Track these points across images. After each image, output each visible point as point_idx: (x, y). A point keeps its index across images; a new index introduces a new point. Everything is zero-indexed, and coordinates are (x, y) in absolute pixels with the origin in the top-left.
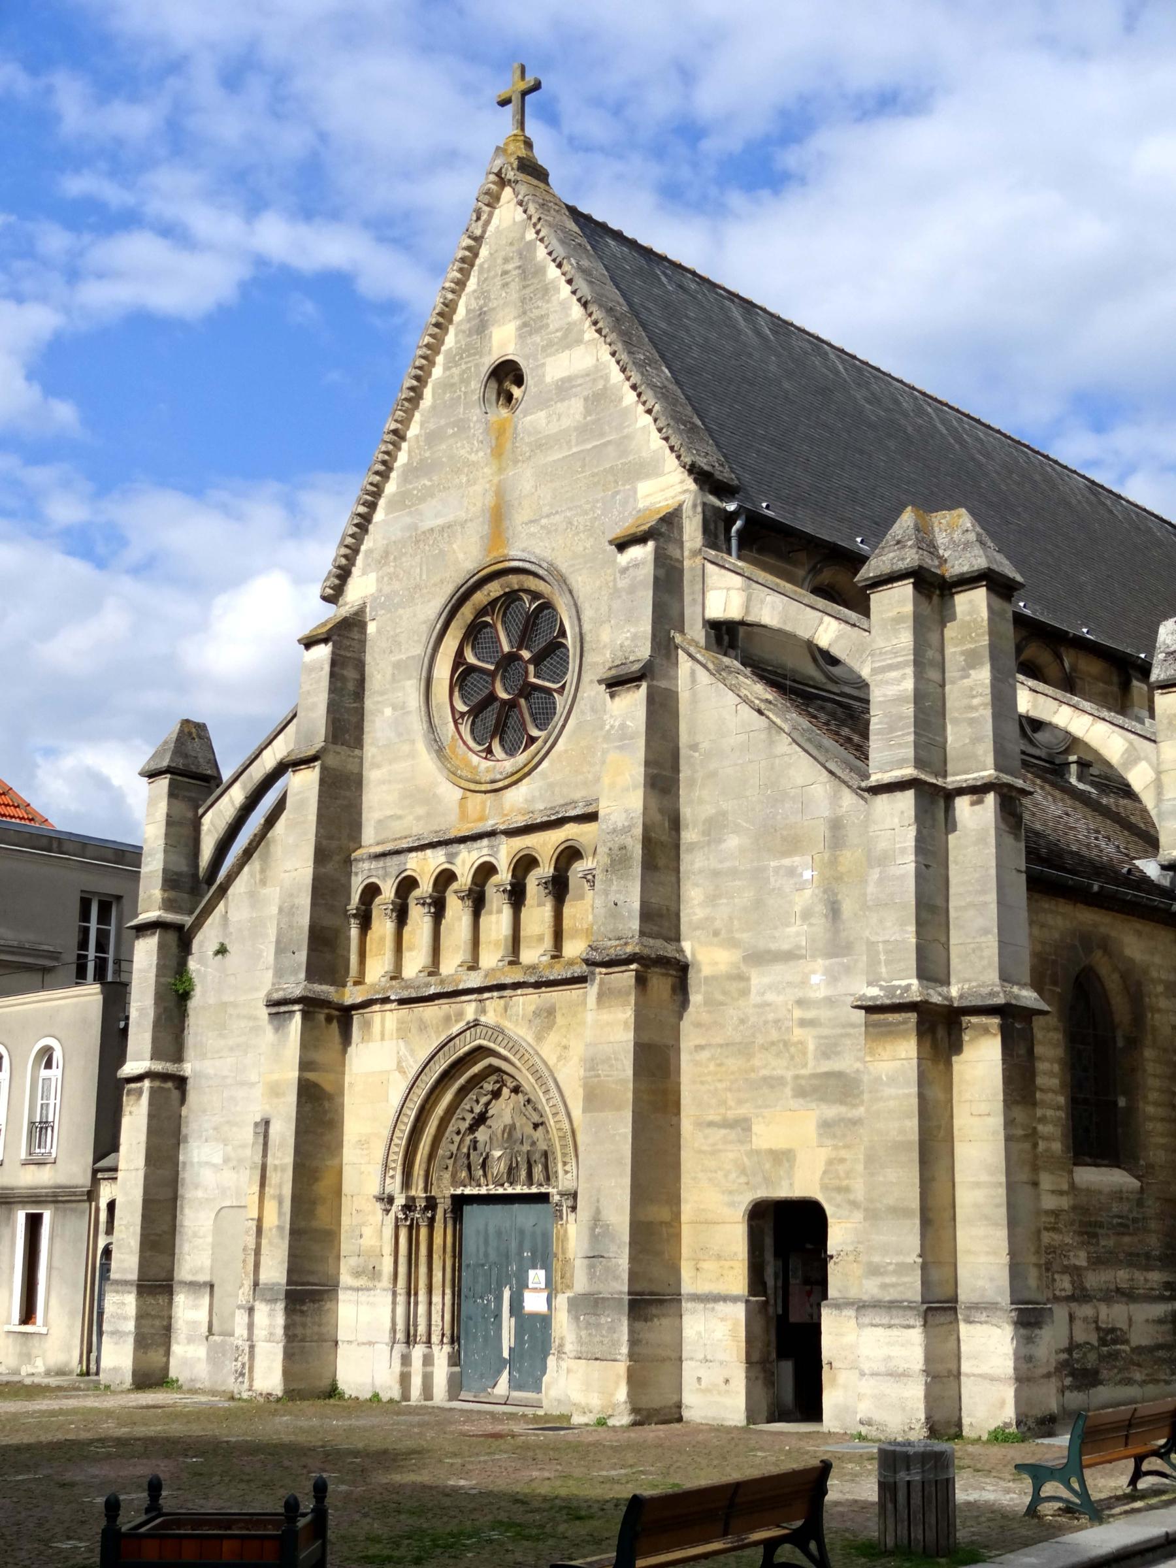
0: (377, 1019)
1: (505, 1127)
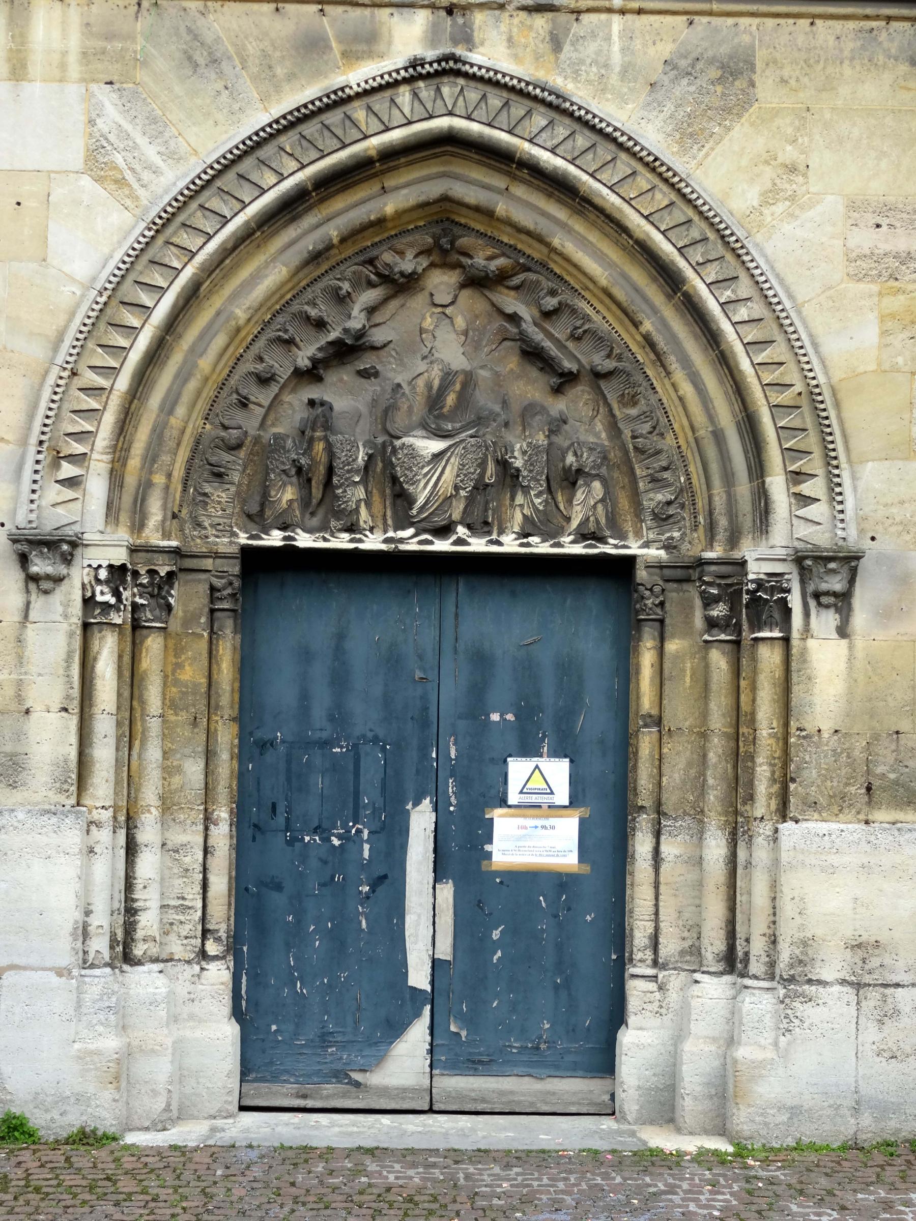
1: (448, 377)
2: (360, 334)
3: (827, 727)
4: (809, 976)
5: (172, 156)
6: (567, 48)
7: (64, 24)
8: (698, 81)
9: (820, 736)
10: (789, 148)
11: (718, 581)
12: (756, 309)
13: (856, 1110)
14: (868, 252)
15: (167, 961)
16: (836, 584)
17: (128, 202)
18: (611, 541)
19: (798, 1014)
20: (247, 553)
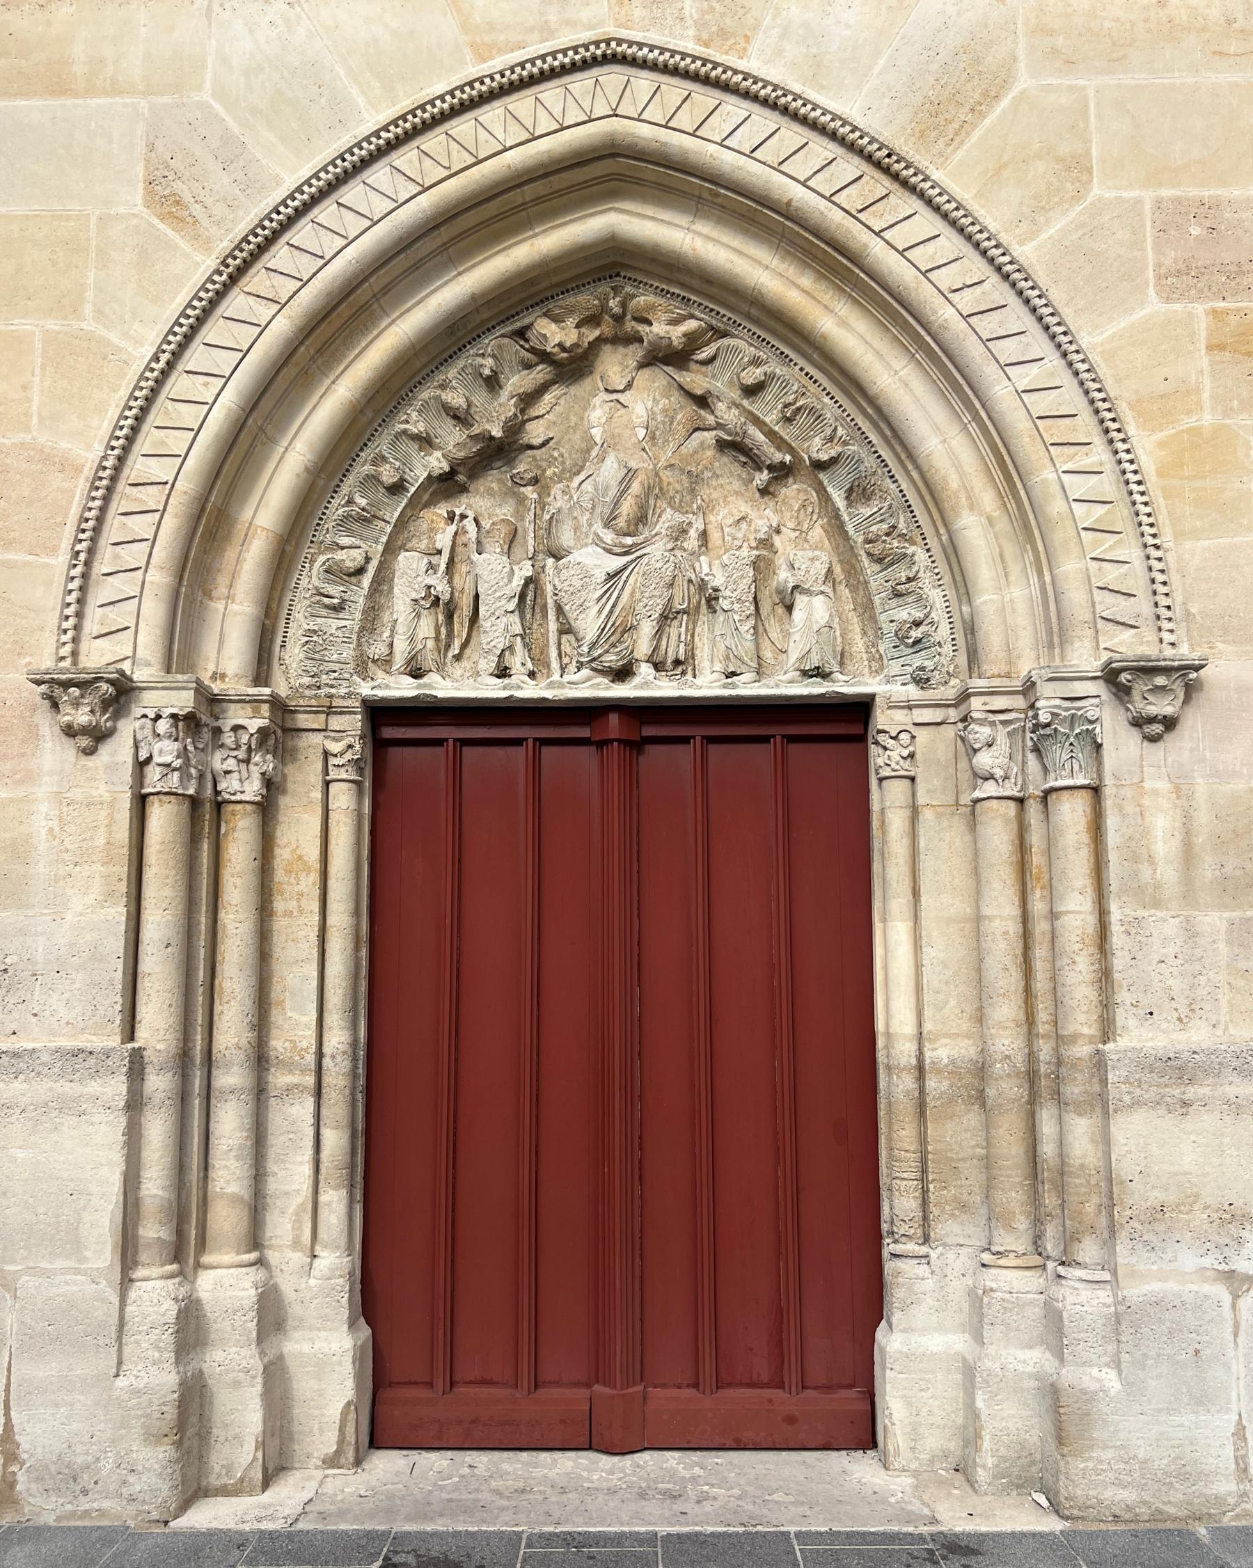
11: (992, 717)
16: (1163, 706)
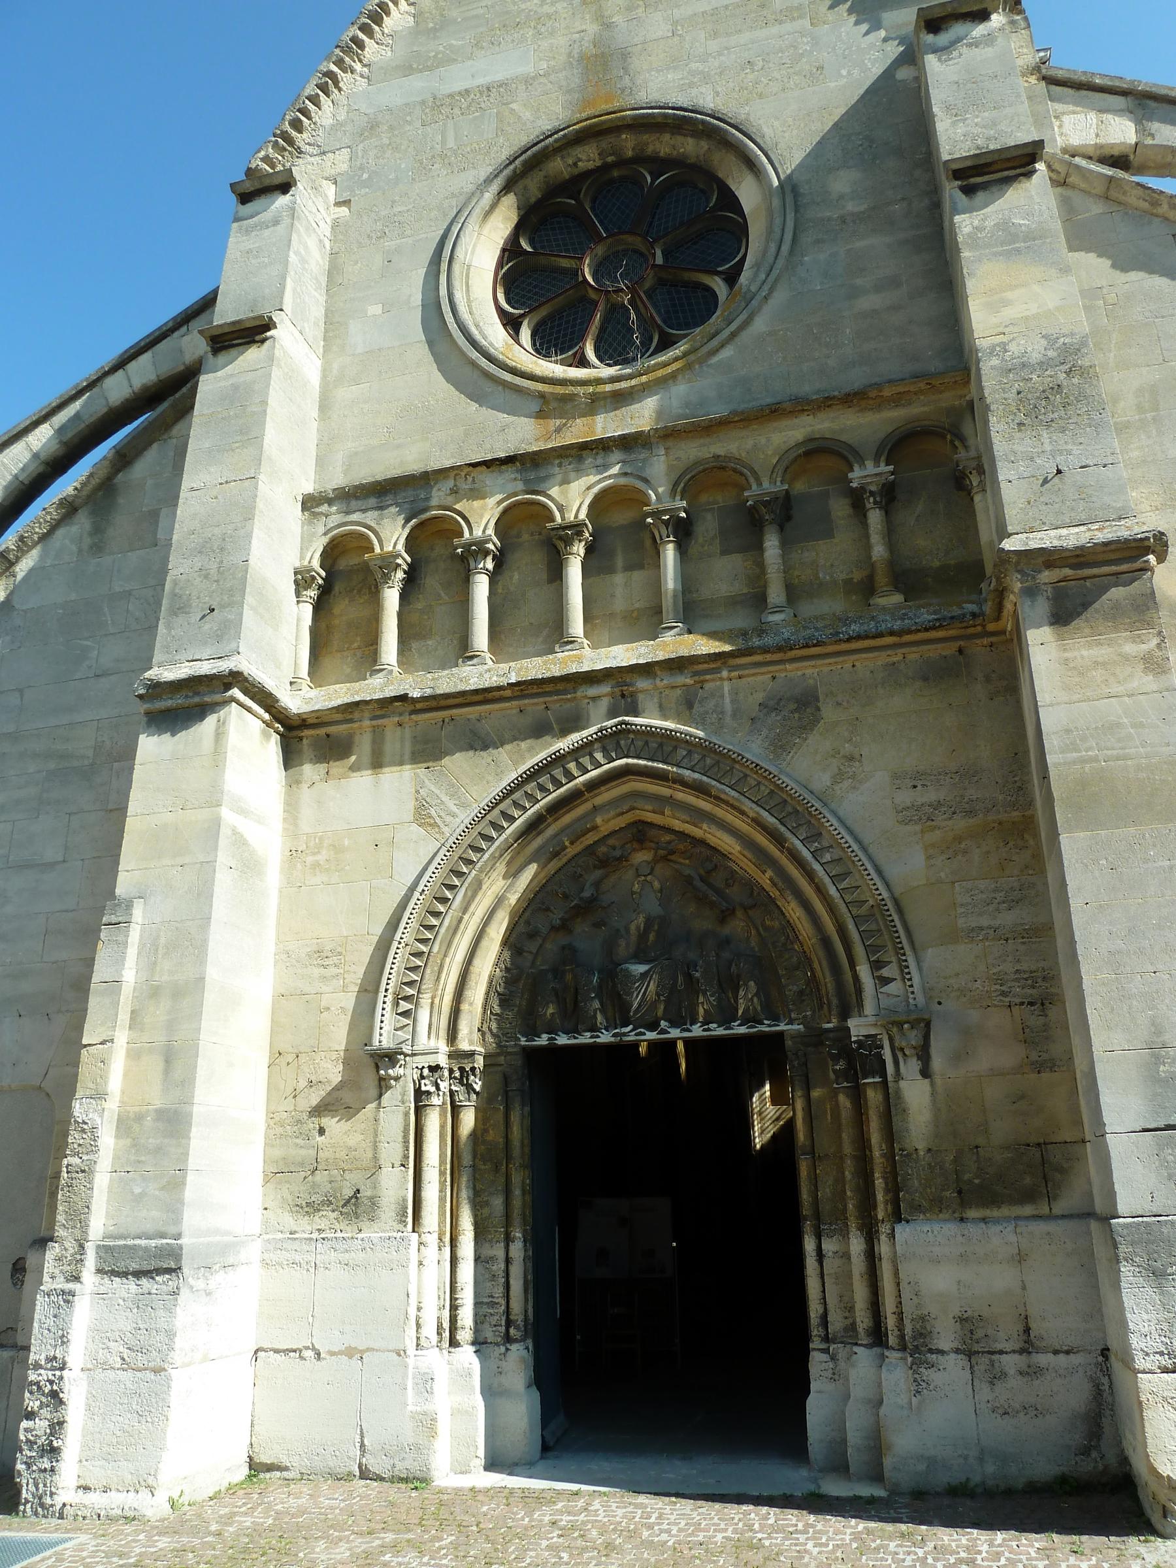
0: (364, 743)
1: (649, 922)
2: (593, 900)
3: (921, 1146)
4: (930, 1346)
5: (463, 805)
6: (696, 705)
7: (402, 739)
8: (783, 713)
9: (917, 1154)
10: (847, 745)
12: (837, 853)
13: (981, 1460)
14: (909, 804)
15: (483, 1343)
17: (437, 836)
18: (766, 1022)
19: (925, 1378)
20: (524, 1048)
